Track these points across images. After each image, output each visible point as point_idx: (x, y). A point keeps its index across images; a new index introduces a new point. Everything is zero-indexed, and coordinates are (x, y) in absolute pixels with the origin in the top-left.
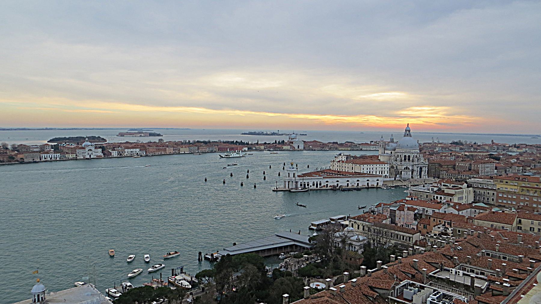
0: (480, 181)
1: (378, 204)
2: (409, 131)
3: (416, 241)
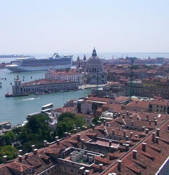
2: (95, 52)
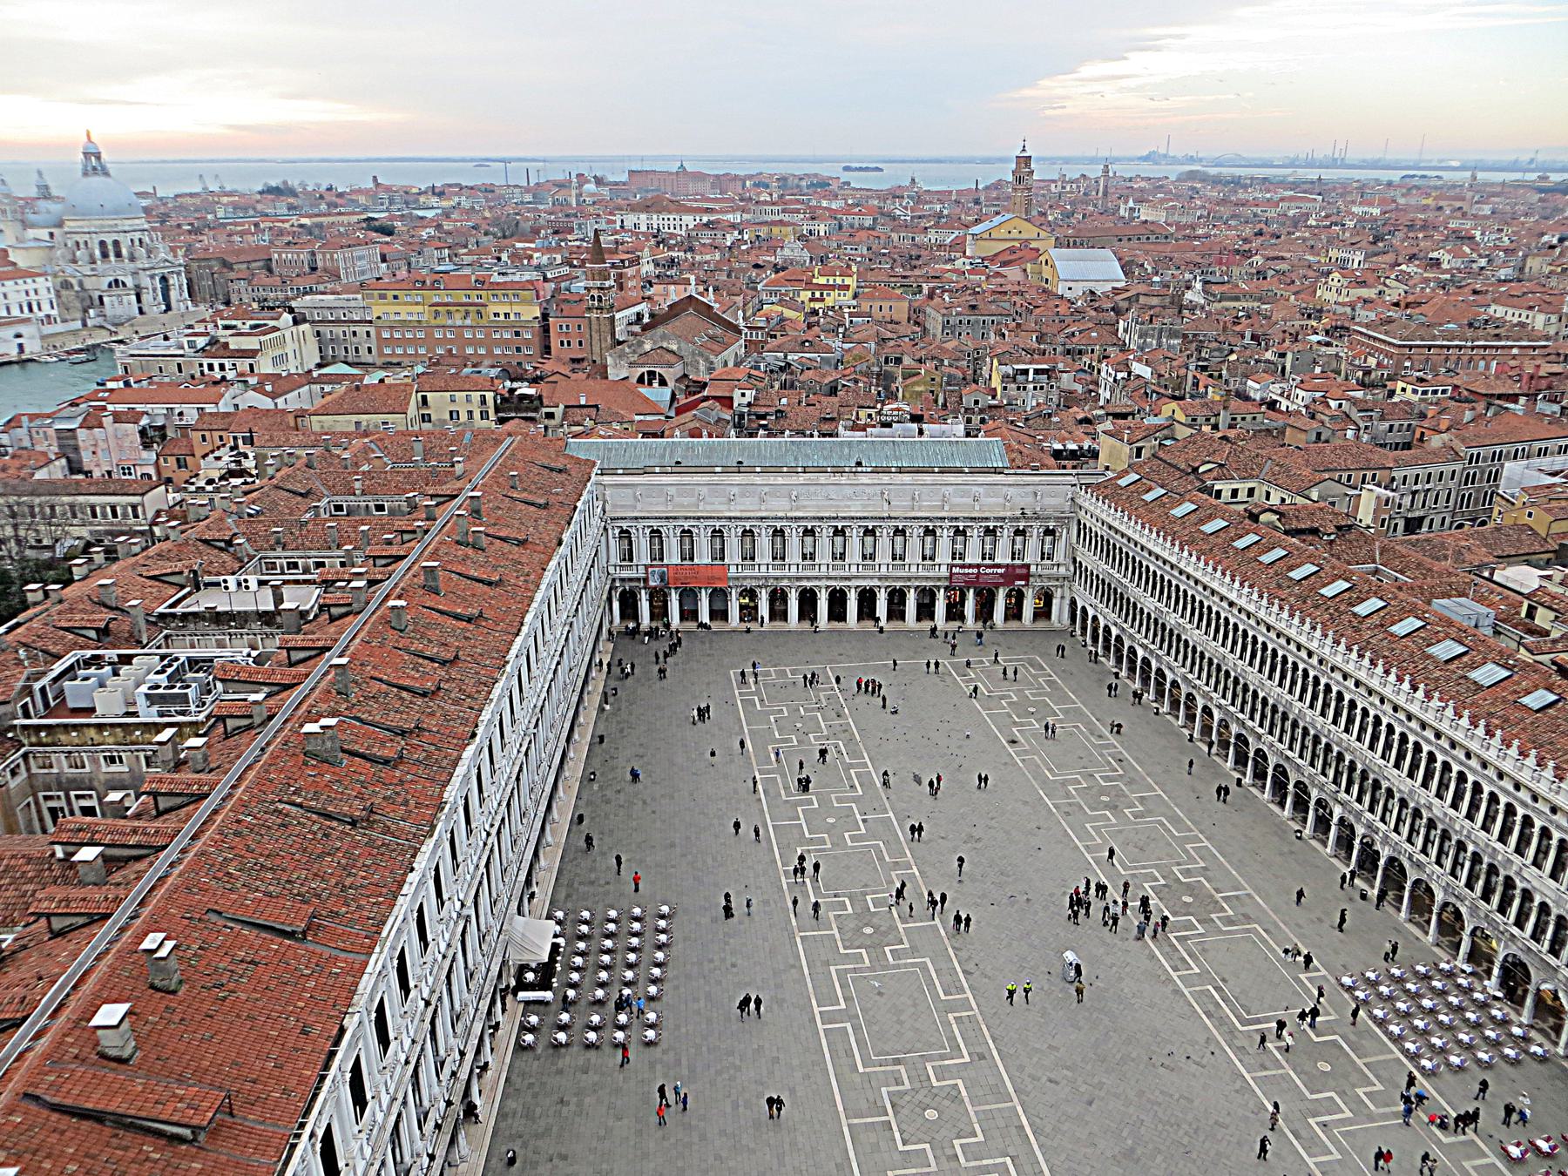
0: (329, 301)
1: (9, 421)
2: (98, 156)
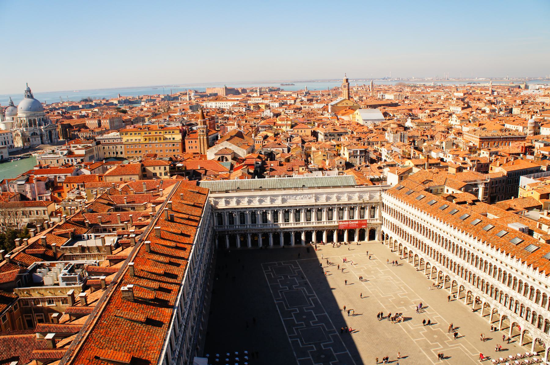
3: (52, 212)
